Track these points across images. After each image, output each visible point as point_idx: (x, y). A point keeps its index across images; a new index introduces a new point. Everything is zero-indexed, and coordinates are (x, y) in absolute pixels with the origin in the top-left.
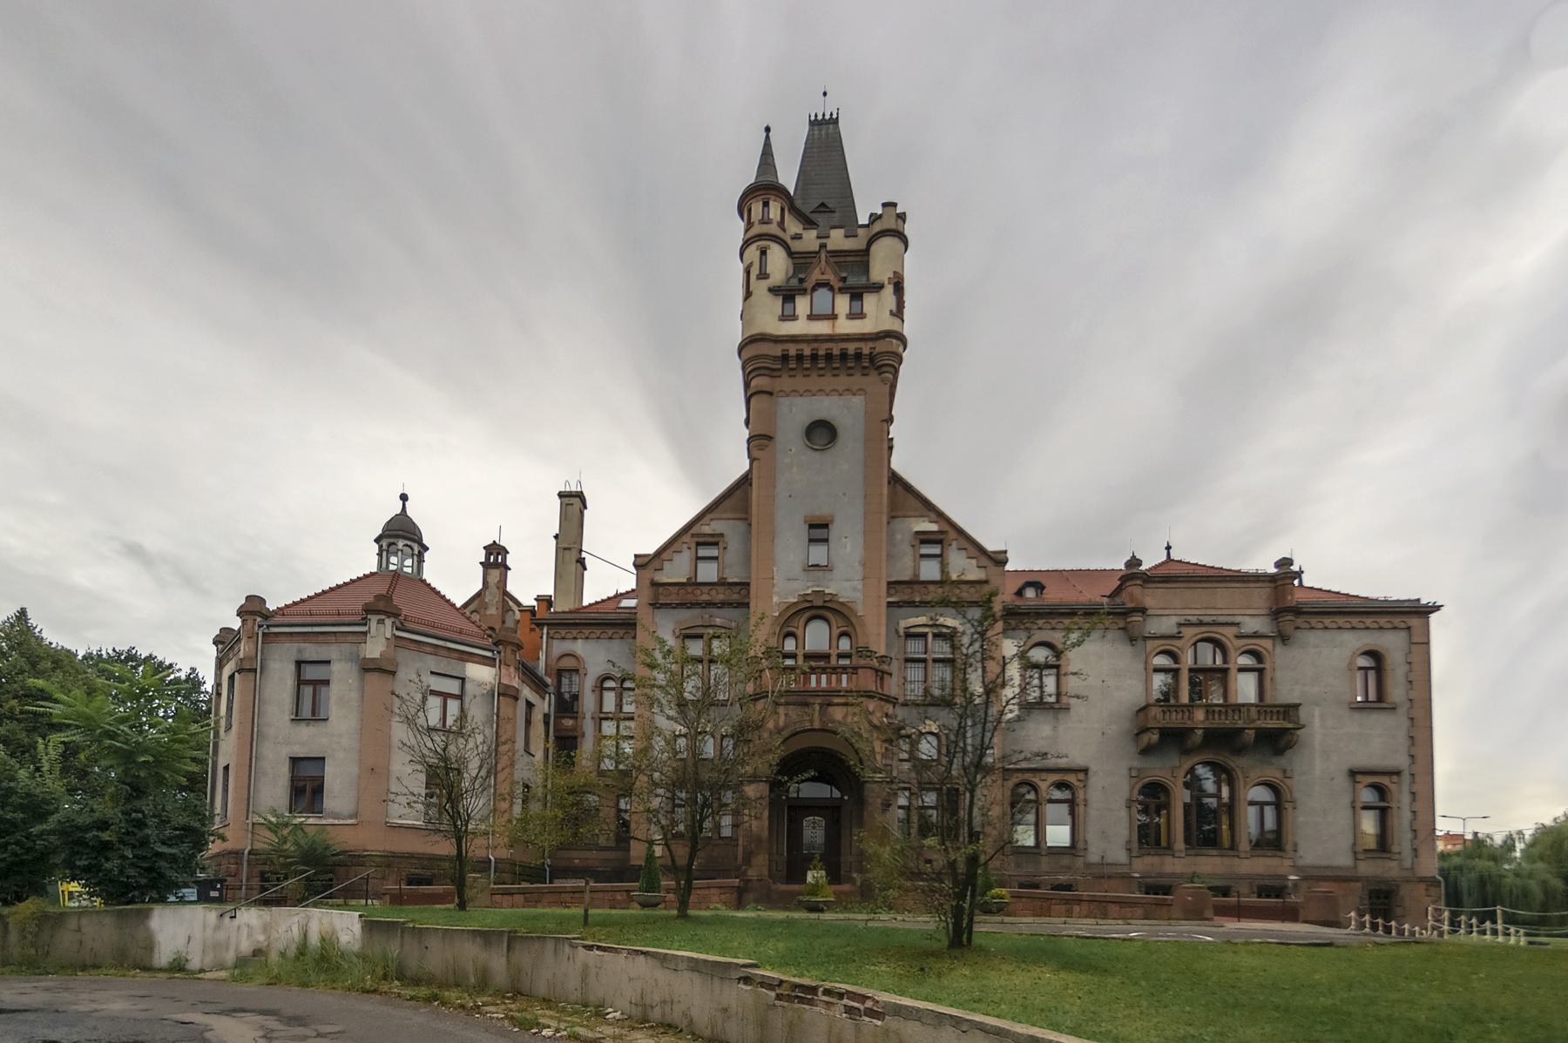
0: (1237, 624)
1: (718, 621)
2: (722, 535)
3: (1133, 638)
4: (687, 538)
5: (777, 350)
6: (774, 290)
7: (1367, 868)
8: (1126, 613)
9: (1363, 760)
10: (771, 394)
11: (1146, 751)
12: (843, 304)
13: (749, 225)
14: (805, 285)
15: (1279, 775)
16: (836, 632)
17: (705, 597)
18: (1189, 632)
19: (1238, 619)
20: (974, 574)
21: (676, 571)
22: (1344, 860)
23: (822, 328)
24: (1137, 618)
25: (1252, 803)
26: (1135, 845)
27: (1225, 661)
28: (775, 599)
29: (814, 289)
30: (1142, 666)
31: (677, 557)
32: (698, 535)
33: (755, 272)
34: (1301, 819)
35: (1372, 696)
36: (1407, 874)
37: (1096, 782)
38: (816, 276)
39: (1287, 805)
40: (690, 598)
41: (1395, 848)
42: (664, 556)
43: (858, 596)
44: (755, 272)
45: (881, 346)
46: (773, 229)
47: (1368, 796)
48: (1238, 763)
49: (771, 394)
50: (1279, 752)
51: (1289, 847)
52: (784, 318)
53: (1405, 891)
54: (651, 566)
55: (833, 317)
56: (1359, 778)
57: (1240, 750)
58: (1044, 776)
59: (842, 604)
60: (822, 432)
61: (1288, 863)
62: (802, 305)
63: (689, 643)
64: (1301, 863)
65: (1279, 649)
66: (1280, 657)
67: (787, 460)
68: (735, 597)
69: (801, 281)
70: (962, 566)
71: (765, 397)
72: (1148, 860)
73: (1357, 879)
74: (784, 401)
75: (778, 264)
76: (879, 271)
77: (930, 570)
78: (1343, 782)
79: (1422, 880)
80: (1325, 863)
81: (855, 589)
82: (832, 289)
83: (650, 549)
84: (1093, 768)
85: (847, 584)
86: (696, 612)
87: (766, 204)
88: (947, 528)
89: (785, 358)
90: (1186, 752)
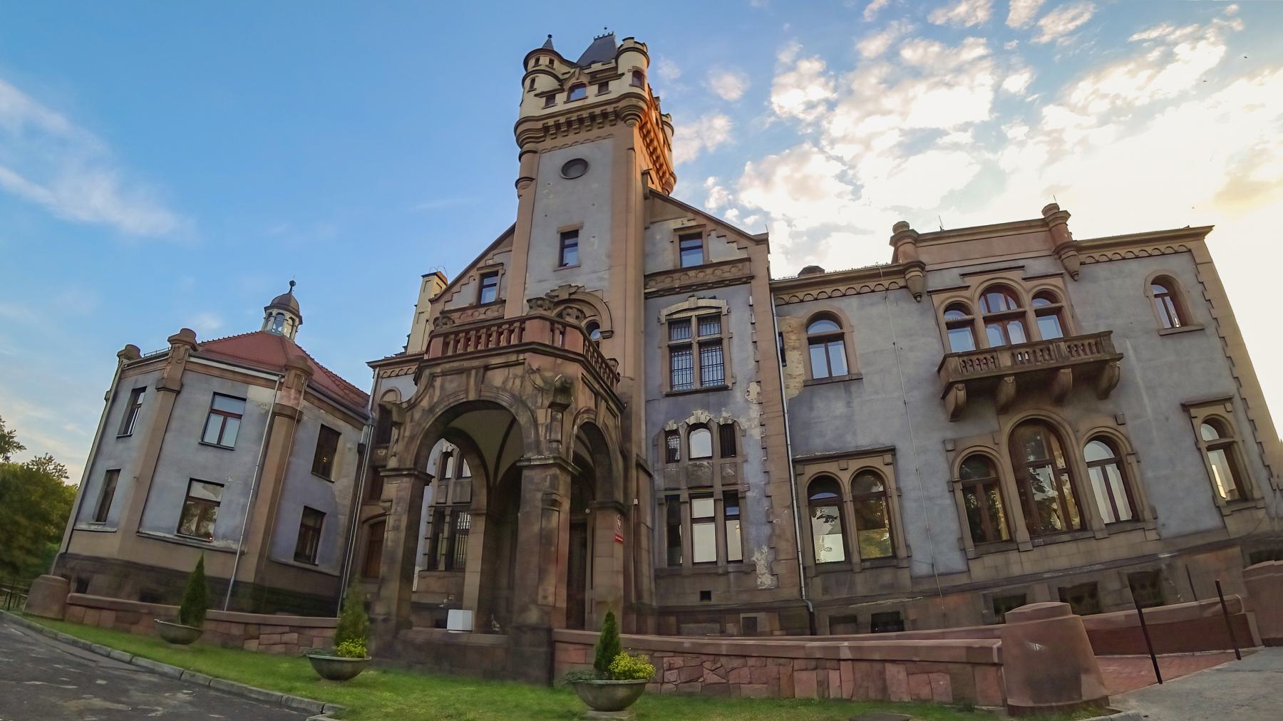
11: (957, 415)
15: (1111, 423)
25: (1091, 464)
26: (969, 542)
27: (1019, 306)
30: (933, 322)
34: (1150, 474)
37: (908, 460)
39: (1131, 459)
48: (1063, 415)
50: (1105, 395)
51: (1147, 515)
56: (1193, 412)
57: (1060, 400)
58: (843, 464)
61: (1152, 535)
64: (1165, 533)
65: (1071, 286)
66: (1071, 295)
70: (718, 250)
72: (989, 560)
78: (1178, 420)
80: (1192, 528)
81: (601, 279)
84: (902, 447)
85: (595, 276)
88: (703, 221)
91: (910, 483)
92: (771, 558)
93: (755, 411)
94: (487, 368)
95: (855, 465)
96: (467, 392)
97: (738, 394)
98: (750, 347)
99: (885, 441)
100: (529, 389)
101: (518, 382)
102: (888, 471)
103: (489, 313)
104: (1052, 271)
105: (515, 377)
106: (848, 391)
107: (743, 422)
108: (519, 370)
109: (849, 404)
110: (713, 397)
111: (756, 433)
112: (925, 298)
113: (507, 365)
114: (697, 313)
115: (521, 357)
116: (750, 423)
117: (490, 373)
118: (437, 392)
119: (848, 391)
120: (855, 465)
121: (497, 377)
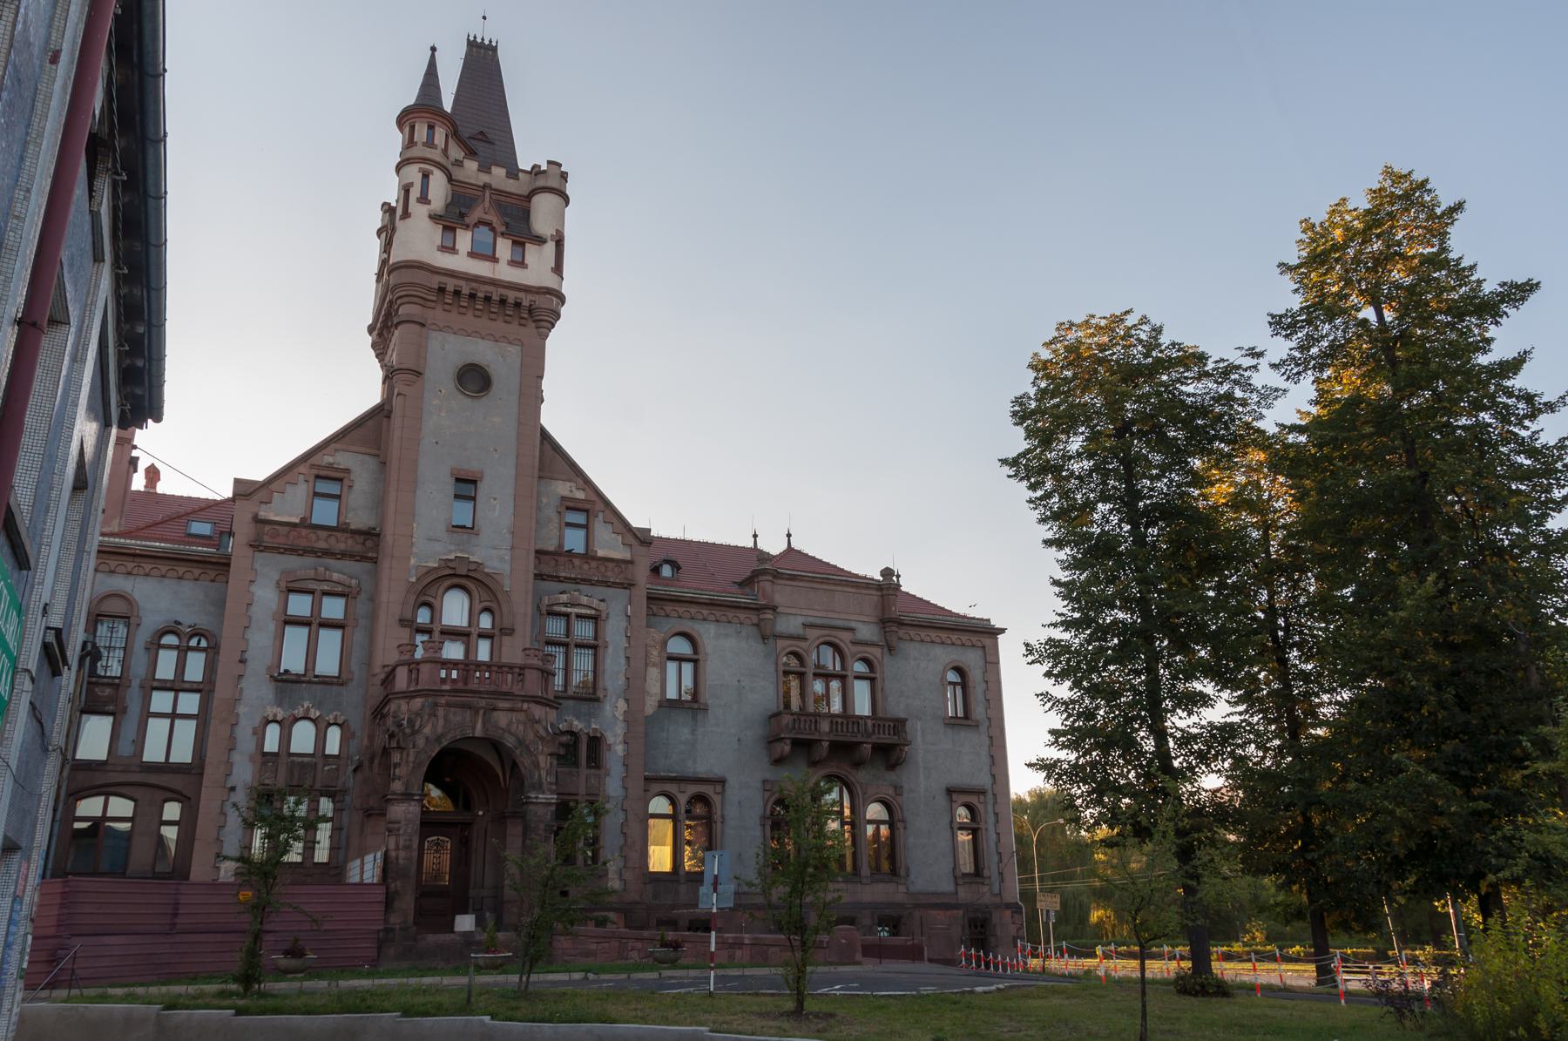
0: (852, 630)
1: (336, 576)
2: (347, 471)
3: (766, 636)
4: (302, 469)
5: (435, 281)
6: (434, 217)
7: (964, 894)
8: (759, 609)
9: (959, 779)
10: (423, 325)
11: (778, 761)
12: (504, 248)
13: (410, 143)
14: (467, 220)
16: (478, 607)
17: (322, 545)
18: (812, 634)
19: (853, 625)
20: (621, 553)
21: (288, 508)
22: (947, 886)
23: (481, 269)
24: (769, 615)
27: (843, 667)
28: (413, 561)
29: (476, 225)
30: (772, 668)
31: (289, 488)
32: (319, 467)
33: (415, 193)
35: (960, 714)
36: (997, 900)
37: (734, 792)
38: (477, 214)
40: (303, 543)
41: (986, 873)
42: (274, 486)
43: (505, 568)
44: (415, 193)
45: (540, 301)
46: (436, 155)
47: (962, 814)
49: (423, 325)
52: (443, 248)
53: (995, 919)
54: (257, 497)
55: (493, 259)
56: (955, 796)
58: (683, 787)
59: (487, 574)
60: (474, 379)
61: (902, 889)
62: (464, 240)
63: (293, 598)
64: (912, 889)
65: (887, 658)
67: (436, 402)
68: (358, 548)
69: (462, 215)
70: (608, 546)
71: (418, 327)
73: (957, 907)
74: (434, 334)
75: (439, 188)
76: (541, 223)
77: (574, 541)
78: (942, 800)
79: (1008, 906)
81: (501, 559)
82: (493, 229)
83: (260, 474)
84: (732, 781)
86: (309, 560)
87: (431, 127)
88: (594, 497)
89: (442, 290)
90: (814, 764)
91: (732, 812)
92: (621, 864)
93: (620, 729)
94: (494, 709)
95: (693, 789)
96: (474, 728)
97: (608, 707)
98: (623, 661)
99: (718, 771)
100: (531, 736)
101: (521, 727)
102: (716, 799)
103: (332, 540)
104: (875, 639)
105: (519, 722)
106: (694, 718)
107: (610, 739)
108: (521, 716)
109: (693, 732)
110: (584, 707)
111: (620, 749)
112: (771, 641)
113: (511, 710)
114: (576, 610)
115: (525, 706)
116: (615, 738)
117: (495, 714)
118: (441, 721)
119: (694, 718)
120: (693, 789)
121: (502, 719)
